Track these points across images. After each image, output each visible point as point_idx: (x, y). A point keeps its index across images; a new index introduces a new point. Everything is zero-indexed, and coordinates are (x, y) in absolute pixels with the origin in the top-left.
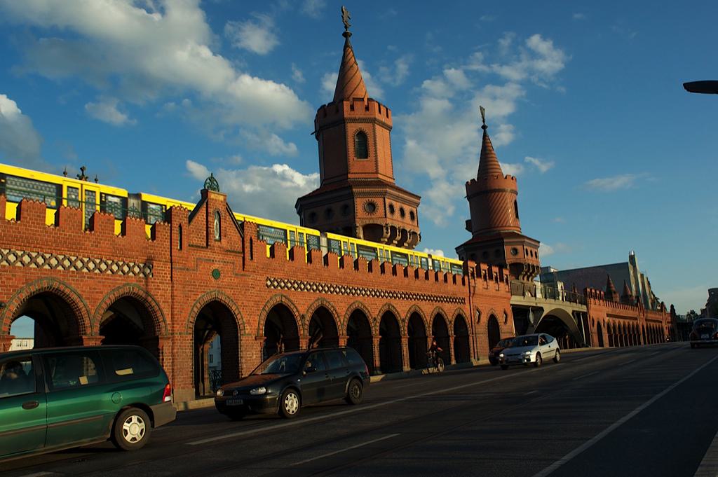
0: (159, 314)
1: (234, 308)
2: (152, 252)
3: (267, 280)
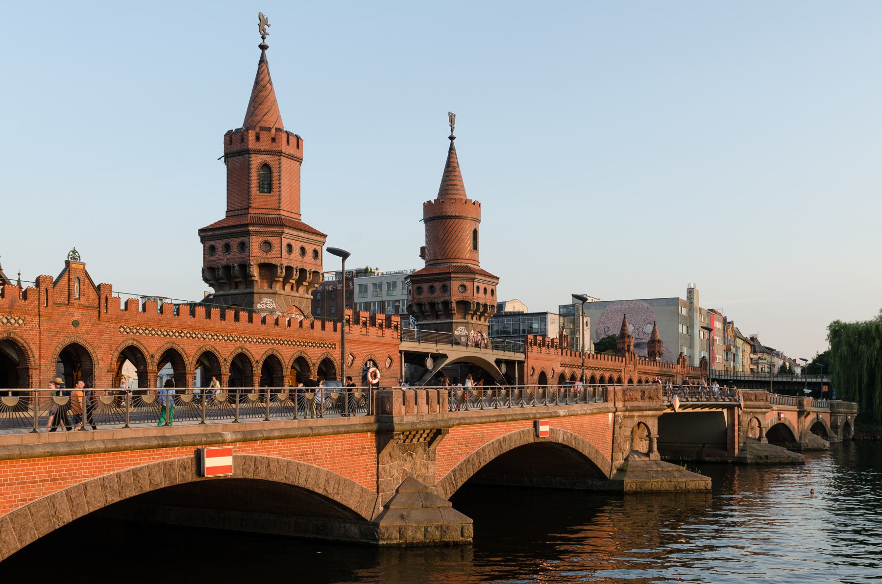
0: (30, 352)
1: (90, 349)
2: (24, 309)
3: (120, 328)
